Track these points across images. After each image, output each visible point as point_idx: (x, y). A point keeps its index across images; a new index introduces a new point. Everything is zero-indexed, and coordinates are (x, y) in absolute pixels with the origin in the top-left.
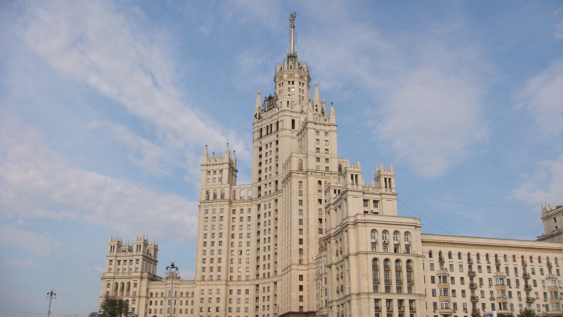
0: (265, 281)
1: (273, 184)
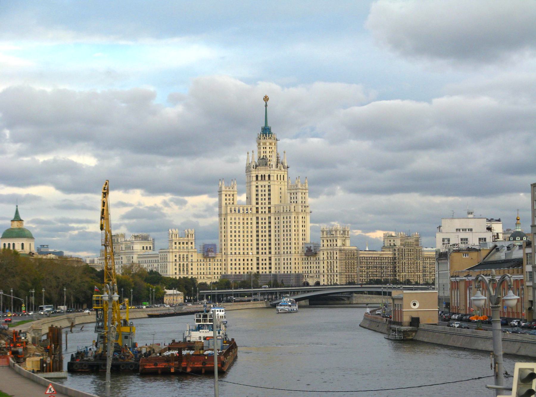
0: (262, 256)
1: (267, 208)
